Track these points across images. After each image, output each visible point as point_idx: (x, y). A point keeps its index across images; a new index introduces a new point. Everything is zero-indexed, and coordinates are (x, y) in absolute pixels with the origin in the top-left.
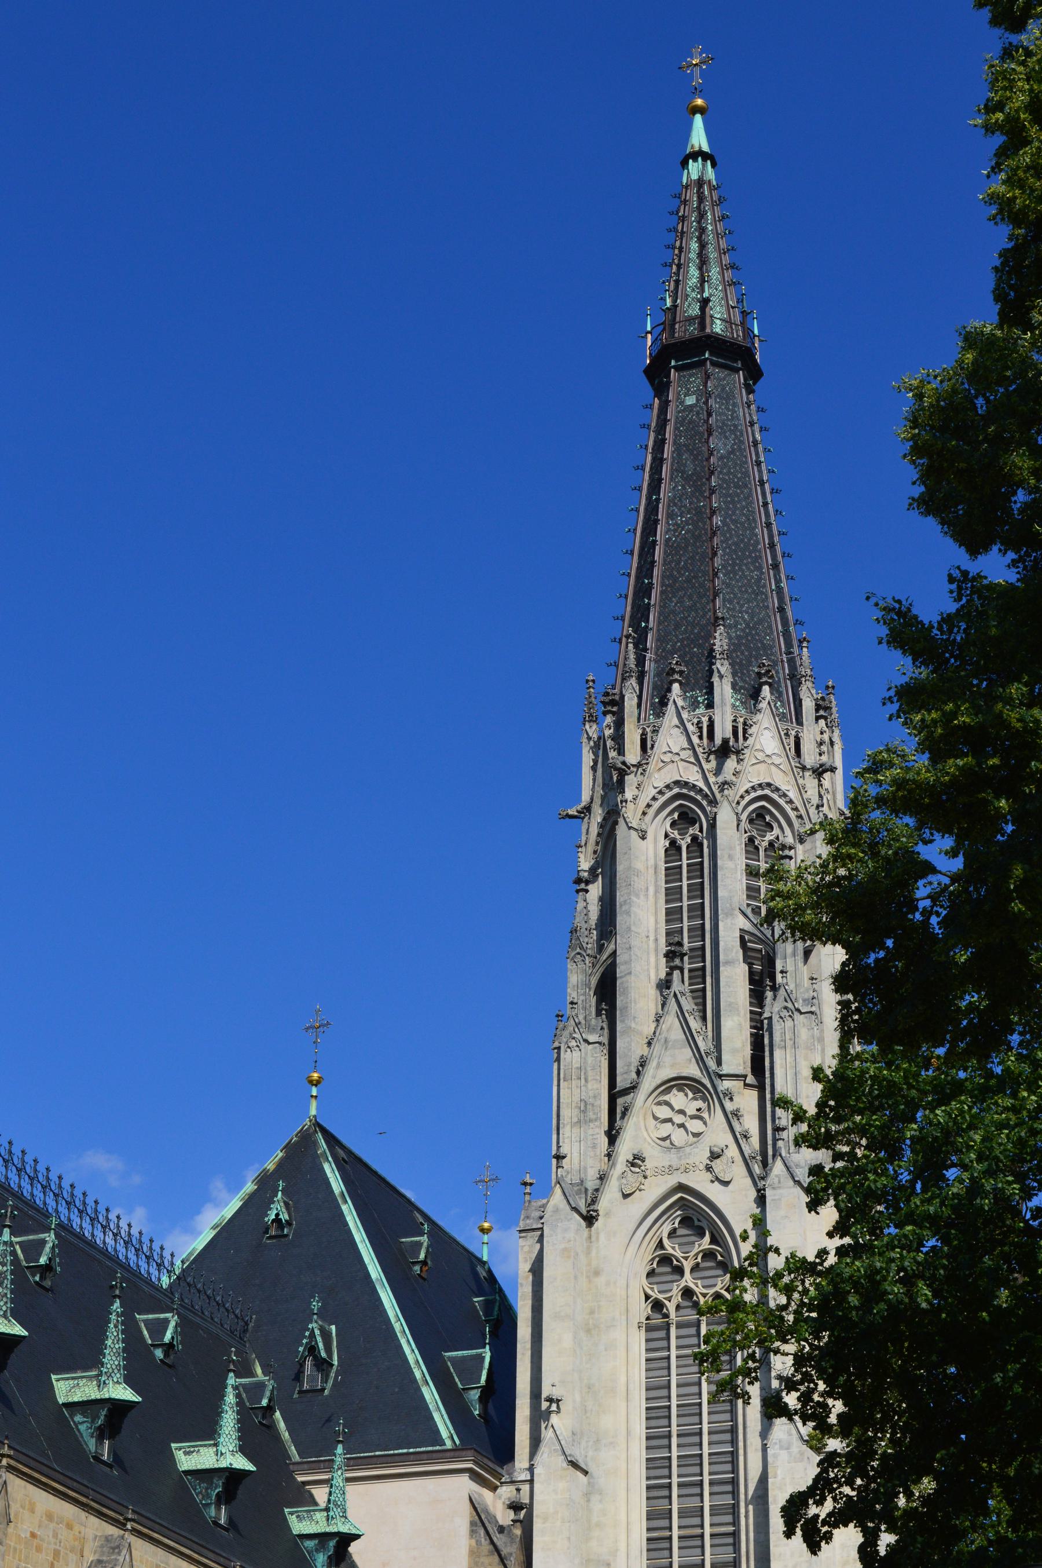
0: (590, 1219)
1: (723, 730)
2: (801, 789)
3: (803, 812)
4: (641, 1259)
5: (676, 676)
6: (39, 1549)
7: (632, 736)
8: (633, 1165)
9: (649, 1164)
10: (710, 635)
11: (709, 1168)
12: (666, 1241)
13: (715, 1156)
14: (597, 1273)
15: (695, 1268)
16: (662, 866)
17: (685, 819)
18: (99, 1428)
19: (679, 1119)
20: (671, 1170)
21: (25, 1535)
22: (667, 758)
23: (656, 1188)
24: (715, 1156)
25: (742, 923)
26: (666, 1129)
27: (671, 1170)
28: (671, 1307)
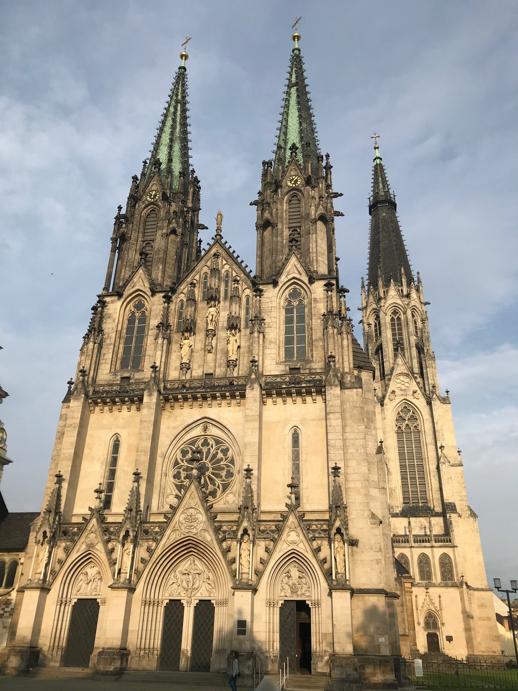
0: (382, 405)
1: (405, 293)
2: (422, 307)
3: (422, 313)
4: (394, 417)
5: (392, 278)
7: (381, 291)
8: (392, 393)
9: (396, 393)
10: (401, 269)
11: (413, 395)
12: (400, 412)
13: (415, 392)
14: (385, 419)
15: (408, 419)
16: (390, 323)
17: (395, 313)
19: (403, 383)
20: (402, 395)
22: (391, 297)
23: (399, 399)
24: (415, 392)
25: (415, 337)
26: (399, 385)
27: (402, 395)
28: (403, 428)
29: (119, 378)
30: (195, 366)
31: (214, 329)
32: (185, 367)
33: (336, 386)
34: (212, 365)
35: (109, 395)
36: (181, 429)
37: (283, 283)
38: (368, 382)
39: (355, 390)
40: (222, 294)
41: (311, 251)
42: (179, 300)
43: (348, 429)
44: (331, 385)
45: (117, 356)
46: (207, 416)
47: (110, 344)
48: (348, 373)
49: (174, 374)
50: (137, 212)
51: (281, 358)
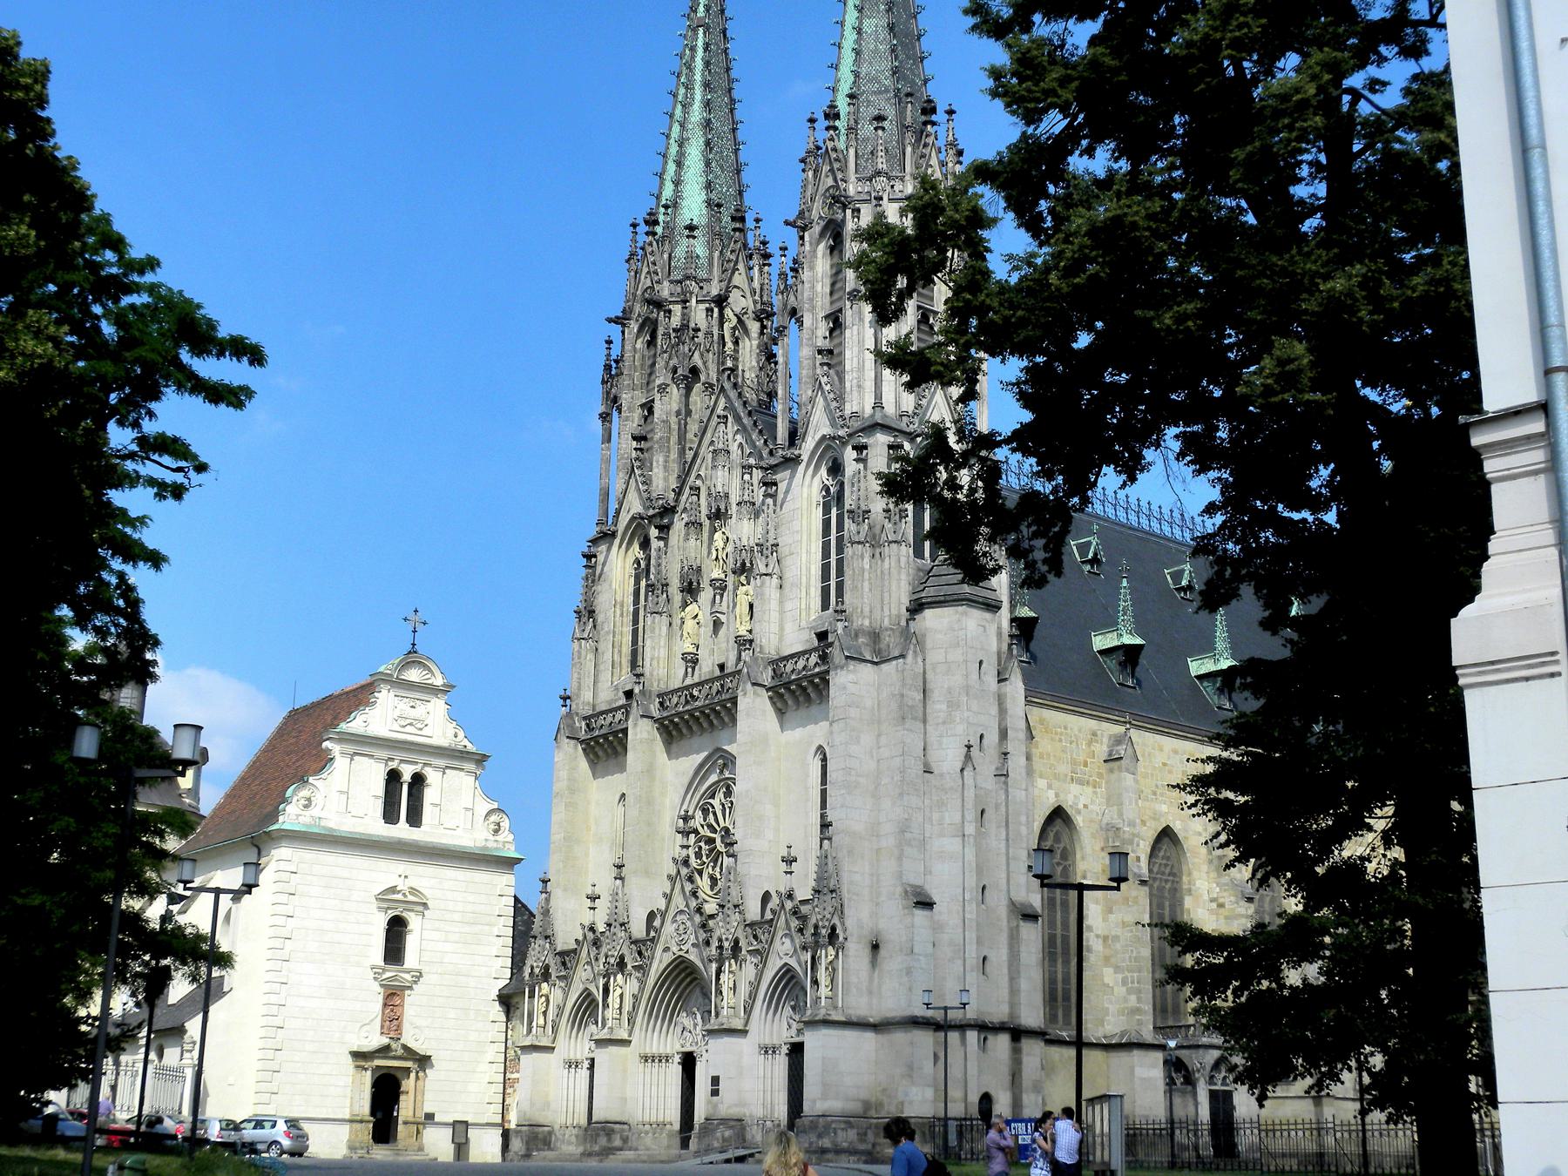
6: (1170, 772)
18: (1218, 689)
21: (1158, 765)
29: (621, 694)
30: (703, 654)
31: (723, 576)
32: (692, 661)
33: (842, 668)
34: (724, 645)
35: (603, 731)
36: (691, 773)
37: (809, 453)
38: (956, 627)
39: (894, 662)
40: (734, 499)
41: (847, 367)
42: (684, 521)
43: (883, 740)
44: (836, 668)
45: (620, 652)
46: (719, 746)
47: (608, 633)
48: (887, 630)
49: (676, 676)
50: (628, 347)
51: (812, 612)
